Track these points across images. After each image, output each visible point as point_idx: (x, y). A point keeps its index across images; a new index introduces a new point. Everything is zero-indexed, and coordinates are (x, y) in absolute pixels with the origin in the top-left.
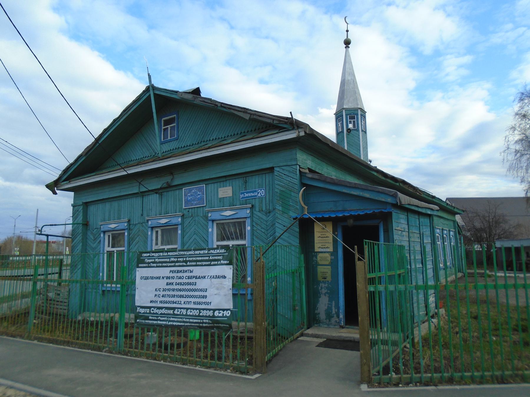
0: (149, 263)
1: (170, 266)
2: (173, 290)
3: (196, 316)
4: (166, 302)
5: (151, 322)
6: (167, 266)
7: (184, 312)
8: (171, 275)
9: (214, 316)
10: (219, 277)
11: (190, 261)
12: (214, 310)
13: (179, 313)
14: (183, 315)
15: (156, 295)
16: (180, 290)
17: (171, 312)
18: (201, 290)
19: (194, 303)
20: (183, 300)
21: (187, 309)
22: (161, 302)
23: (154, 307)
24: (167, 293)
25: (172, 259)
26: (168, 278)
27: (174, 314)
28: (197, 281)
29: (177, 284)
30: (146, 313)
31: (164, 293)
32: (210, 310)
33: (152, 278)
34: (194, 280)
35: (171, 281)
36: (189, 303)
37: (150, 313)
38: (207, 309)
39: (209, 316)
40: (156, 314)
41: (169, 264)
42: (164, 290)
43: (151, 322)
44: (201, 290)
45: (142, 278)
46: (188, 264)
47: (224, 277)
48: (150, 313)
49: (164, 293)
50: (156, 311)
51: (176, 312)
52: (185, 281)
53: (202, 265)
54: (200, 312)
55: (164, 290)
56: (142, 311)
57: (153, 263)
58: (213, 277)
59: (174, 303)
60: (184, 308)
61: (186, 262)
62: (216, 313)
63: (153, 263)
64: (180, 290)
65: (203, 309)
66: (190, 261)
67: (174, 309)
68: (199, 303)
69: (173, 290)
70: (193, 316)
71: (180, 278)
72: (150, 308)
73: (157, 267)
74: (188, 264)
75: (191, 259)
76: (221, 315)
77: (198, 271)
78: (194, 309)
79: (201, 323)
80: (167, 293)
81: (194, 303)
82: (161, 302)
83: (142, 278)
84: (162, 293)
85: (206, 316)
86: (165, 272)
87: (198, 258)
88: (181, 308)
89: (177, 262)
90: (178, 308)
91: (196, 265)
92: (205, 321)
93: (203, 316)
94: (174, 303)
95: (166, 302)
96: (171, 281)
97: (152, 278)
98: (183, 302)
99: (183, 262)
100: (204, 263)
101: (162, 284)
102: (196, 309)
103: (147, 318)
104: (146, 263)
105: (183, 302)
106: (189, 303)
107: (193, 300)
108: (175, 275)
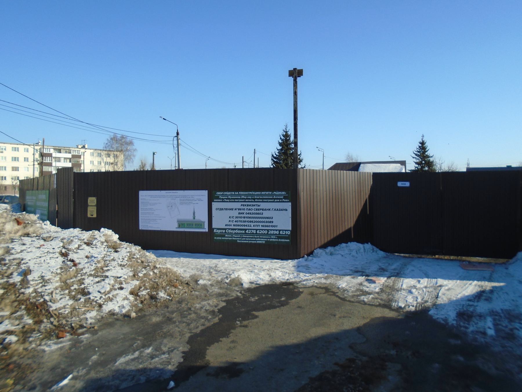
0: (223, 199)
1: (241, 202)
2: (245, 217)
3: (265, 234)
4: (239, 226)
5: (226, 238)
6: (239, 202)
7: (254, 232)
8: (242, 207)
9: (279, 234)
10: (282, 210)
11: (257, 199)
12: (280, 231)
13: (250, 232)
14: (253, 233)
15: (230, 221)
16: (250, 218)
17: (244, 232)
18: (268, 218)
19: (263, 226)
20: (252, 224)
21: (257, 230)
22: (234, 225)
23: (229, 229)
24: (239, 219)
25: (243, 197)
26: (239, 209)
27: (245, 233)
28: (263, 212)
29: (246, 214)
30: (222, 233)
31: (237, 219)
32: (276, 230)
33: (226, 209)
34: (261, 211)
35: (242, 211)
36: (257, 226)
37: (225, 232)
38: (274, 230)
39: (276, 234)
40: (231, 233)
41: (240, 200)
42: (236, 217)
43: (226, 238)
44: (268, 218)
45: (217, 209)
46: (256, 200)
47: (286, 210)
48: (225, 232)
49: (237, 219)
50: (230, 231)
51: (247, 232)
52: (253, 211)
53: (267, 202)
54: (268, 232)
55: (236, 217)
56: (219, 231)
57: (226, 199)
58: (278, 210)
59: (245, 226)
60: (254, 230)
61: (254, 199)
62: (281, 232)
63: (226, 199)
64: (250, 218)
65: (271, 230)
66: (257, 199)
67: (246, 230)
68: (267, 226)
69: (245, 217)
70: (262, 234)
71: (250, 210)
72: (225, 229)
73: (230, 202)
74: (256, 200)
75: (258, 197)
76: (284, 233)
77: (263, 205)
78: (262, 230)
79: (269, 238)
80: (239, 219)
81: (263, 226)
82: (234, 225)
83: (217, 209)
84: (235, 220)
85: (273, 234)
86: (238, 205)
87: (265, 197)
88: (251, 229)
89: (247, 199)
90: (249, 229)
91: (263, 202)
92: (272, 237)
93: (271, 234)
94: (245, 226)
95: (239, 226)
96: (242, 211)
97: (226, 209)
98: (252, 226)
99: (252, 199)
100: (269, 200)
101: (235, 213)
102: (265, 230)
103: (224, 236)
104: (220, 199)
105: (252, 226)
106: (257, 226)
107: (261, 224)
108: (245, 207)
